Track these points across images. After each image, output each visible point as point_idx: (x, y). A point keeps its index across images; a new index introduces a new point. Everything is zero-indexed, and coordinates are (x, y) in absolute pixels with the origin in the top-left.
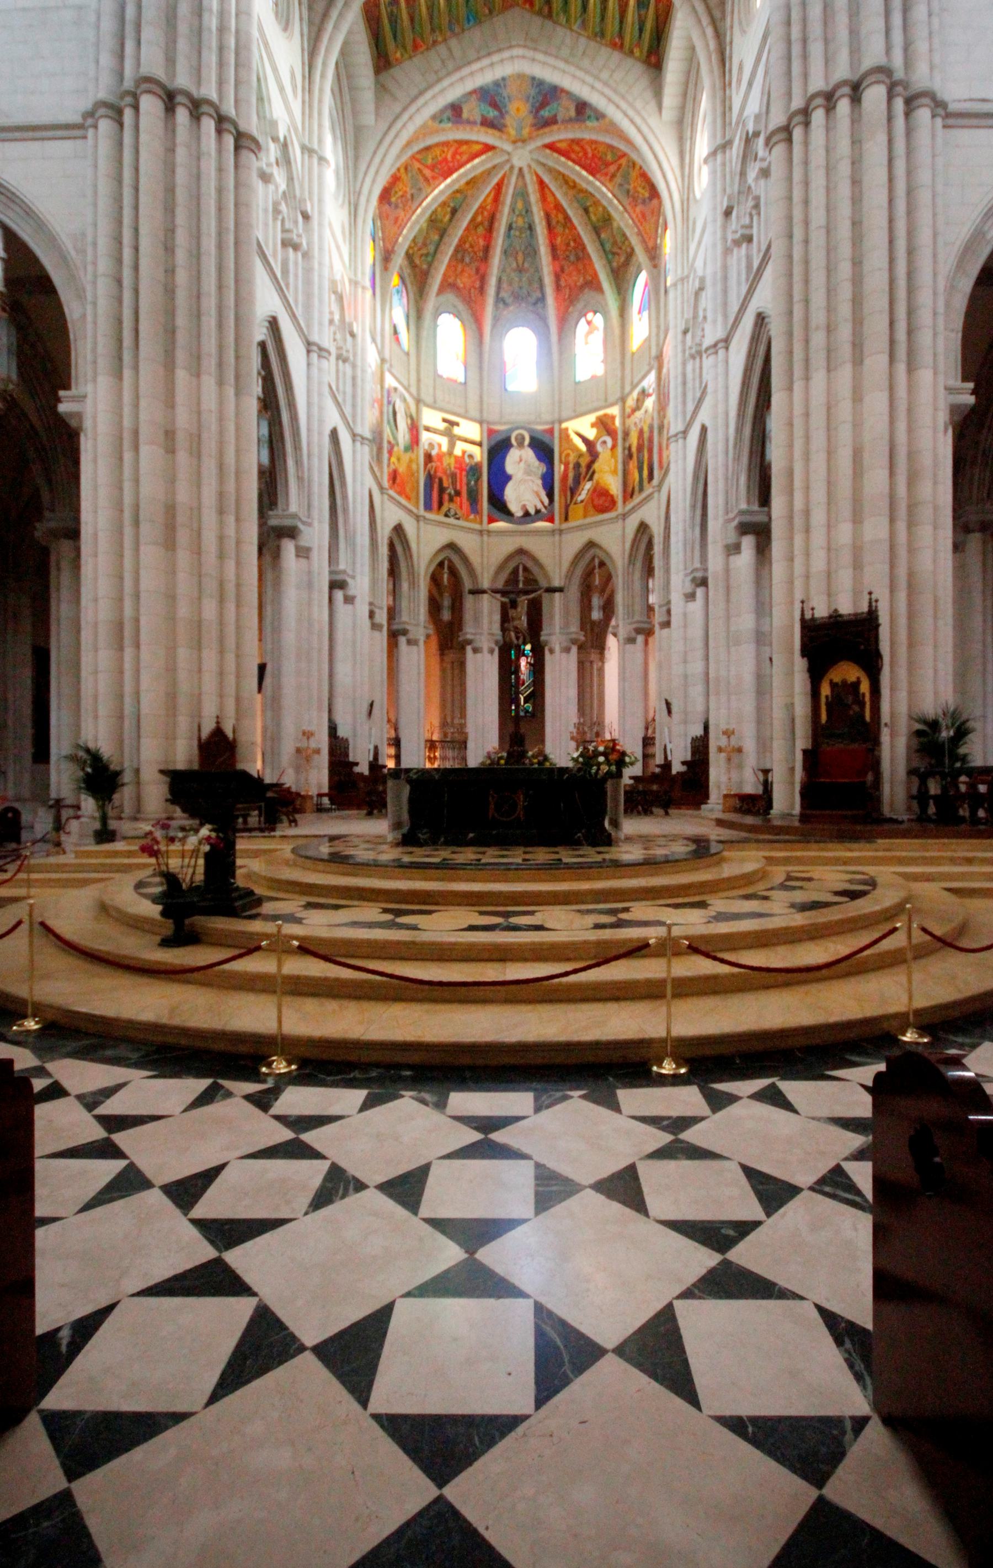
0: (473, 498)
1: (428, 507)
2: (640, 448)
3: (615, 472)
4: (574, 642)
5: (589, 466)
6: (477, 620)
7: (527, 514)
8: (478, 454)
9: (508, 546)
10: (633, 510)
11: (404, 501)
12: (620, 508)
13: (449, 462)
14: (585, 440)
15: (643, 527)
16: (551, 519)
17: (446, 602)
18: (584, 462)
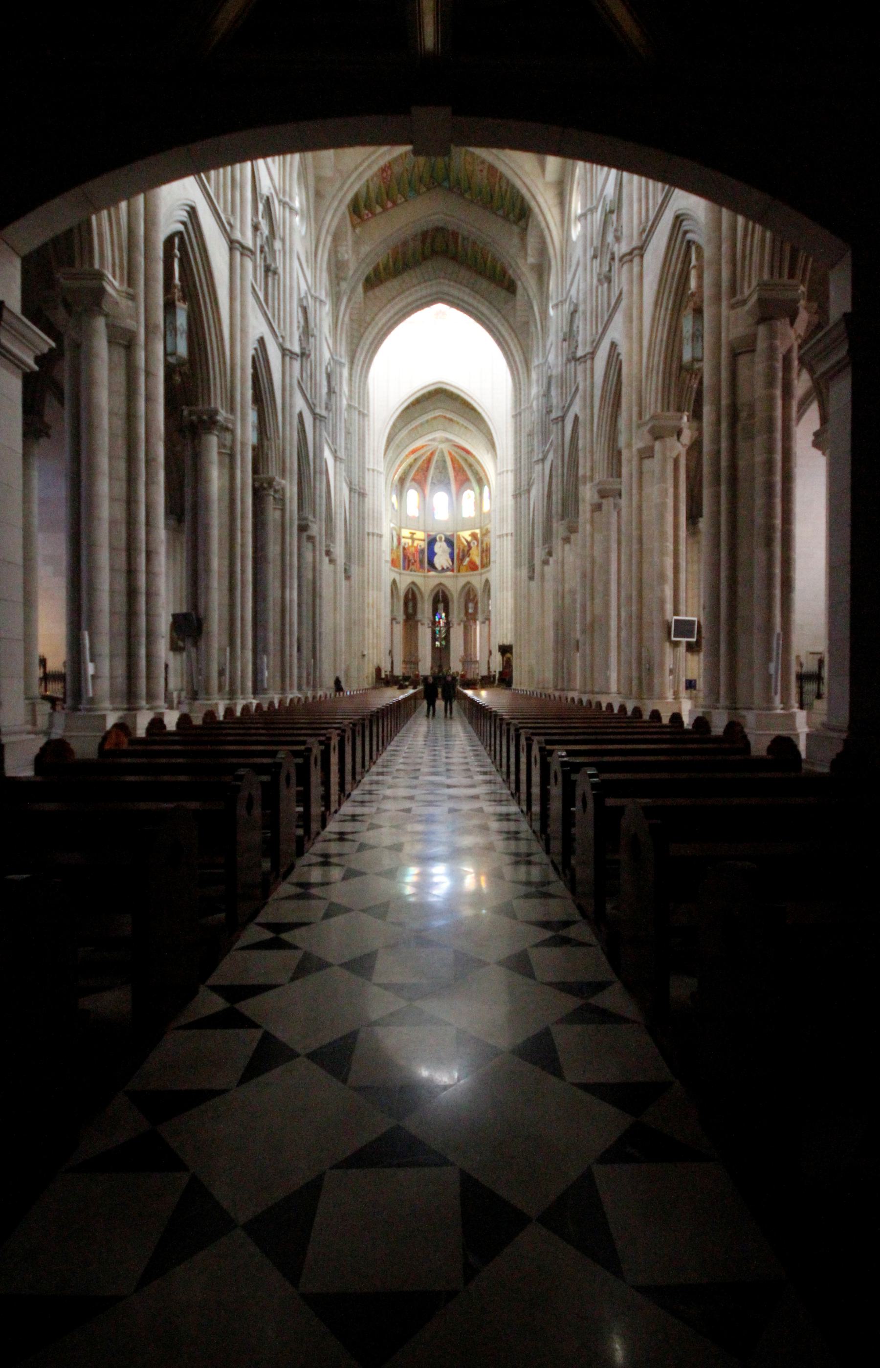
0: (421, 562)
1: (404, 569)
2: (486, 551)
3: (478, 555)
4: (461, 621)
5: (468, 551)
6: (423, 613)
7: (443, 569)
8: (423, 545)
9: (436, 581)
10: (485, 573)
11: (396, 569)
12: (480, 571)
13: (412, 550)
14: (467, 541)
15: (487, 581)
16: (453, 571)
17: (410, 605)
18: (466, 549)
